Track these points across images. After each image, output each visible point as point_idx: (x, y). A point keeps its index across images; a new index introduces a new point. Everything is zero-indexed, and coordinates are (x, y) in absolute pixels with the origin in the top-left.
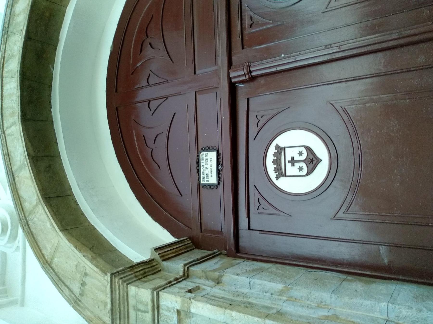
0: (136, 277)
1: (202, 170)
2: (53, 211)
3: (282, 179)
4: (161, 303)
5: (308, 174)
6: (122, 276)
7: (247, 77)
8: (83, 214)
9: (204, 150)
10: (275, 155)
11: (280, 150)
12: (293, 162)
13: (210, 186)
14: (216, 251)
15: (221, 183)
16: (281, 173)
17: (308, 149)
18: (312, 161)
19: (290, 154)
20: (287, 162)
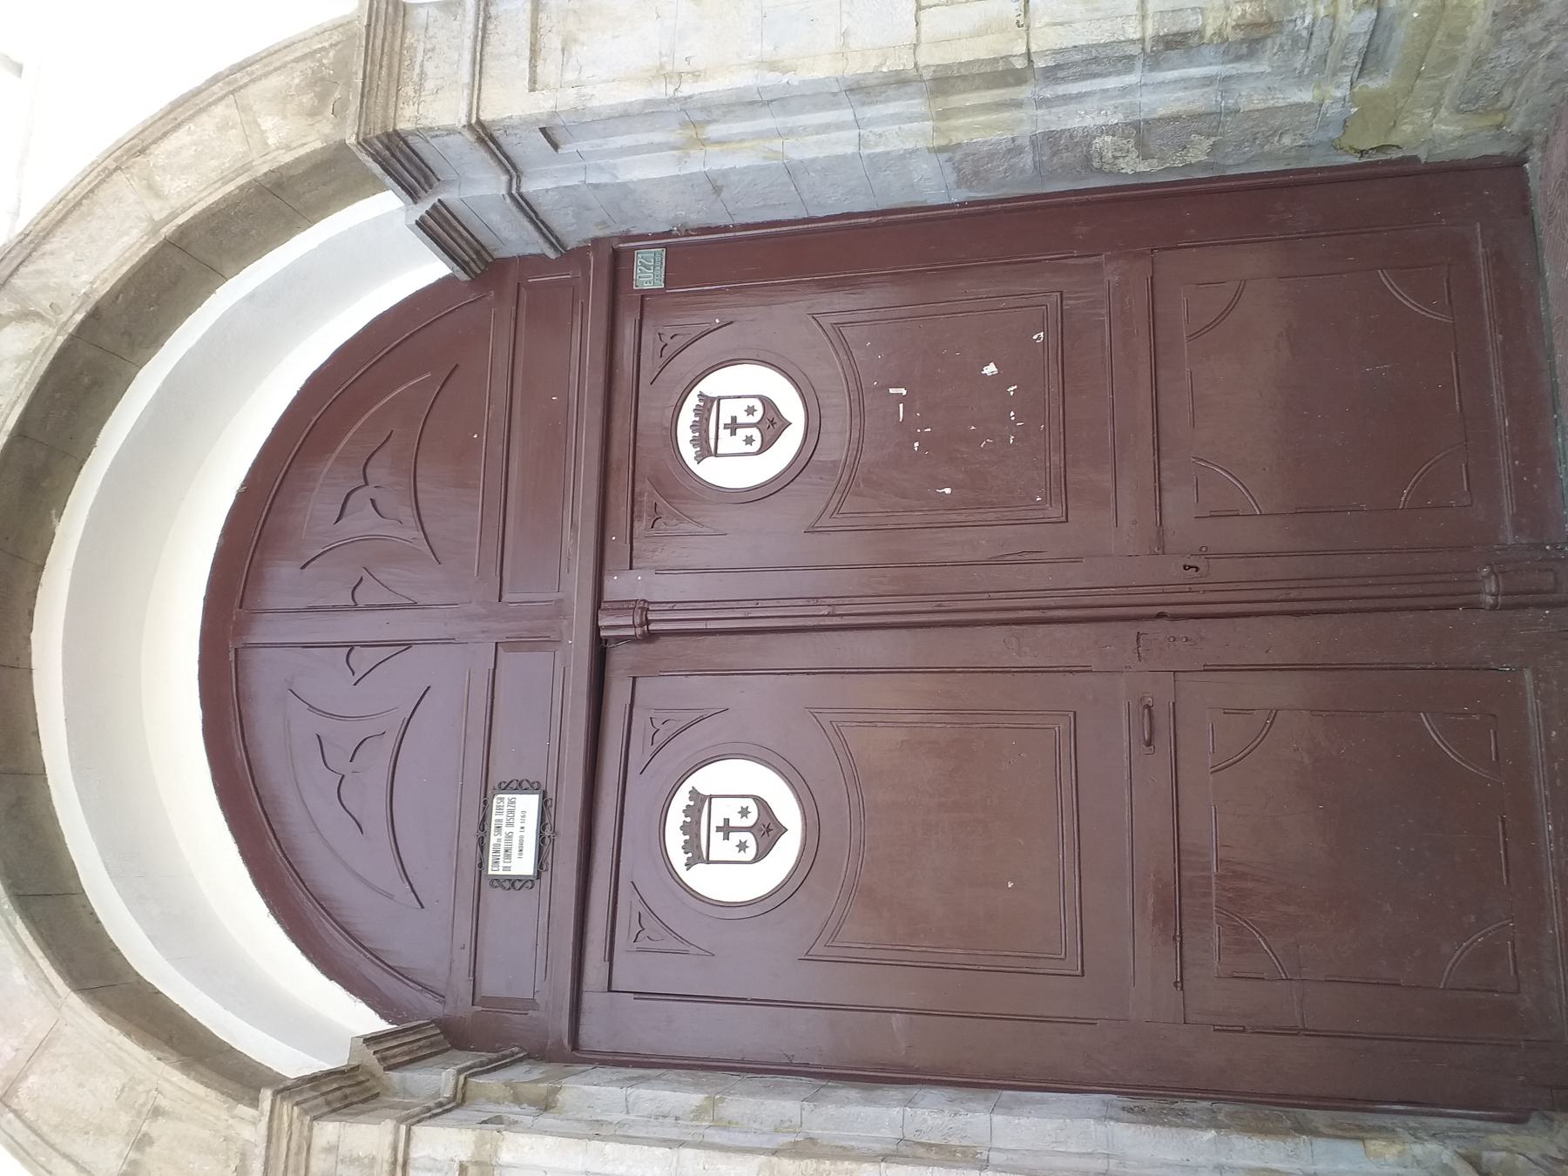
0: (328, 1103)
1: (493, 840)
2: (41, 934)
3: (699, 868)
4: (413, 1154)
5: (757, 859)
6: (298, 1099)
7: (639, 631)
8: (116, 949)
9: (506, 788)
10: (688, 811)
11: (699, 802)
12: (726, 829)
13: (514, 883)
14: (516, 1049)
15: (546, 876)
16: (697, 854)
18: (768, 831)
20: (713, 829)
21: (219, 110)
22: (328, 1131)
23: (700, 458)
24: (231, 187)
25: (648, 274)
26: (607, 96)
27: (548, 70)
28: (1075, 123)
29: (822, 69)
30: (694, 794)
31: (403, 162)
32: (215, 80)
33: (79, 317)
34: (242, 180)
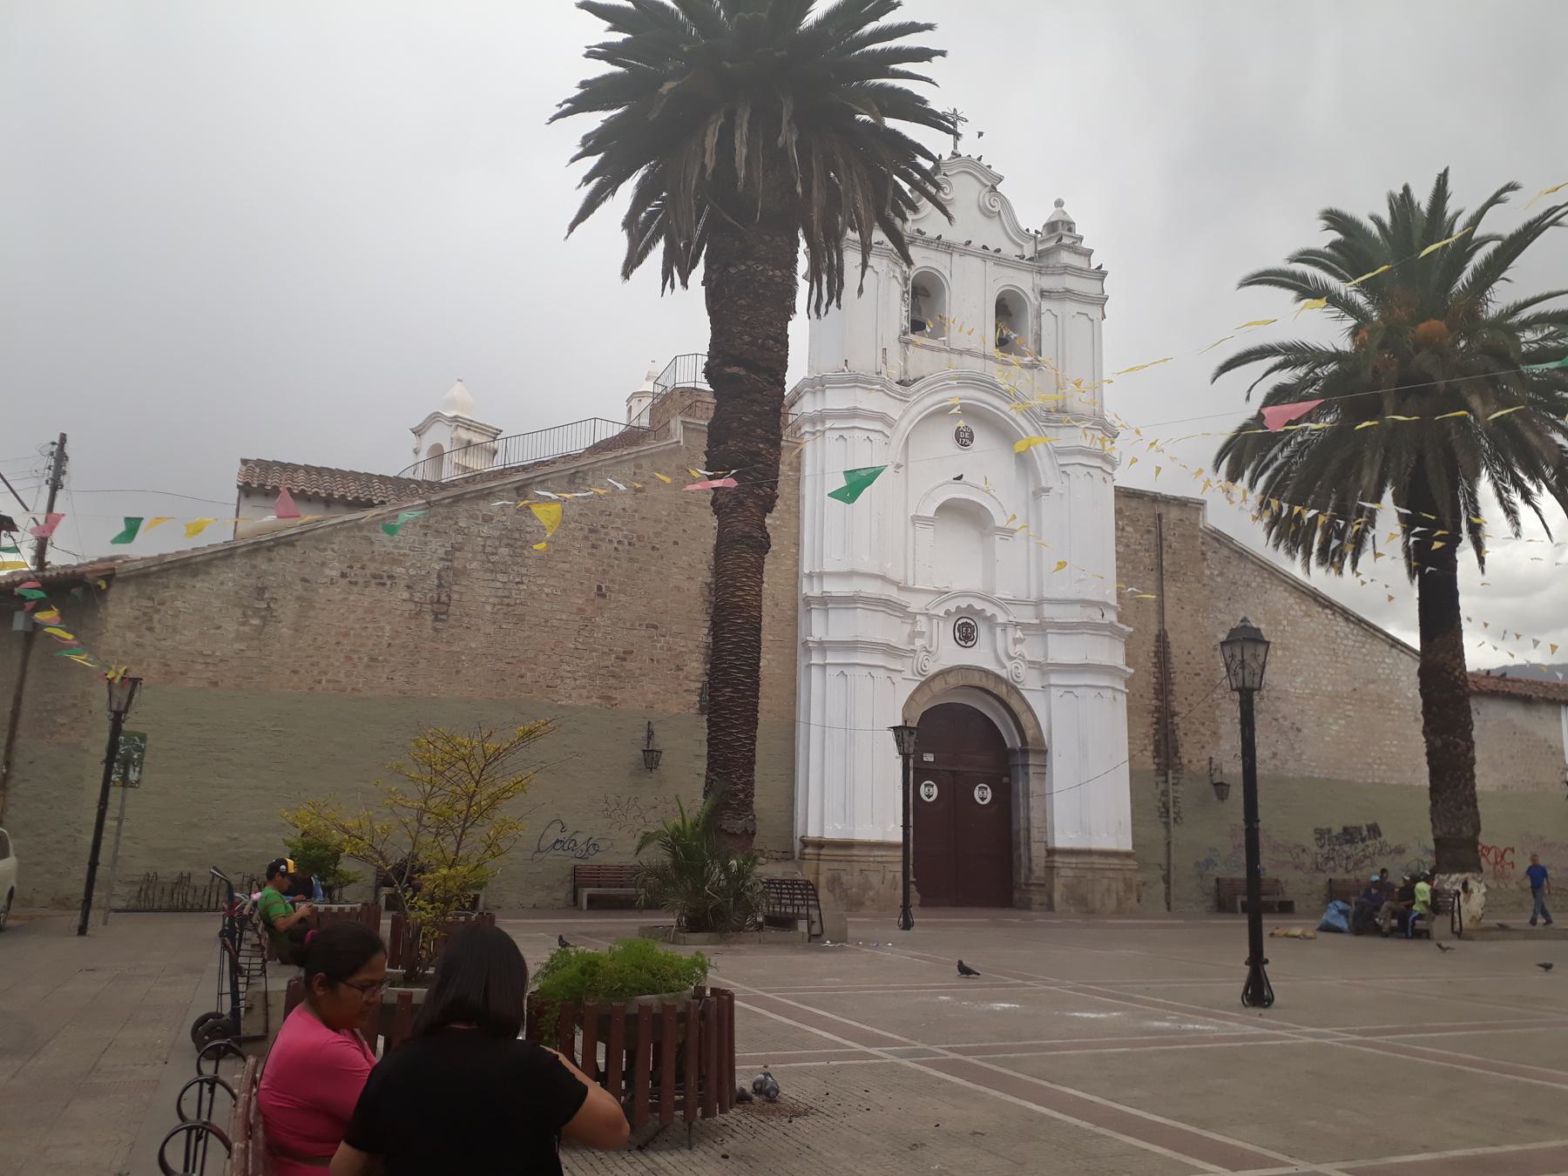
25: (1005, 780)
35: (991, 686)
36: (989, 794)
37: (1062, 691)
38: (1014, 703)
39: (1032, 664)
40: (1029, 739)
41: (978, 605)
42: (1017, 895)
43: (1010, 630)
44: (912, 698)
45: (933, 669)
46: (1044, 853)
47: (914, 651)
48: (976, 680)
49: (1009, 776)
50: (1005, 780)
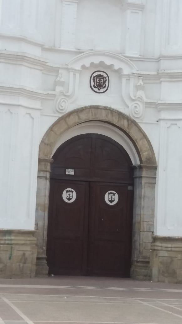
11: (72, 192)
12: (69, 195)
16: (67, 192)
17: (72, 198)
18: (69, 199)
19: (71, 194)
21: (149, 147)
22: (49, 164)
23: (108, 193)
24: (139, 149)
25: (130, 188)
26: (143, 191)
27: (147, 185)
28: (136, 236)
29: (142, 212)
30: (73, 191)
31: (140, 167)
32: (152, 147)
33: (127, 132)
34: (140, 151)
35: (115, 121)
36: (116, 198)
37: (169, 123)
38: (133, 133)
39: (148, 105)
40: (143, 159)
41: (108, 62)
42: (136, 269)
43: (133, 81)
44: (51, 129)
45: (69, 107)
46: (151, 240)
47: (54, 95)
48: (103, 116)
49: (133, 184)
50: (130, 188)
